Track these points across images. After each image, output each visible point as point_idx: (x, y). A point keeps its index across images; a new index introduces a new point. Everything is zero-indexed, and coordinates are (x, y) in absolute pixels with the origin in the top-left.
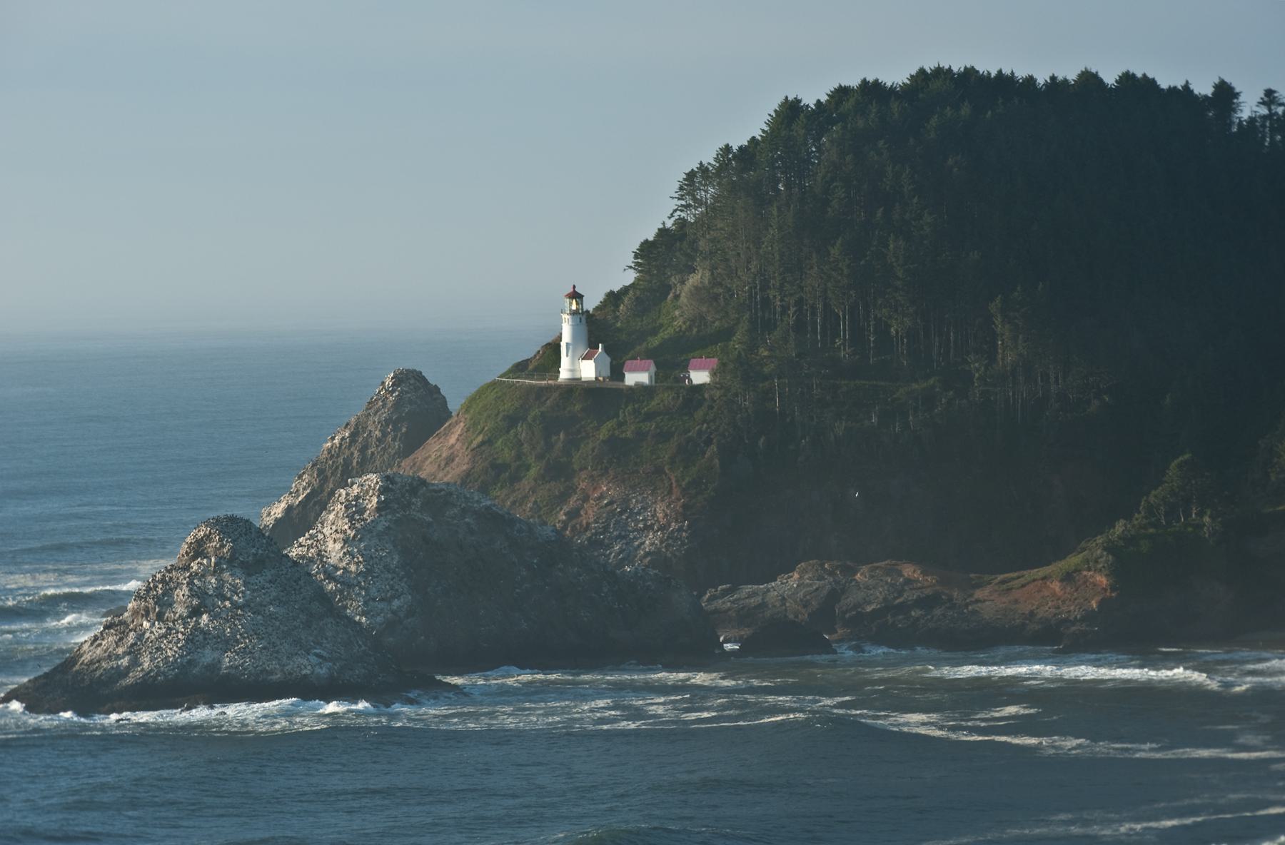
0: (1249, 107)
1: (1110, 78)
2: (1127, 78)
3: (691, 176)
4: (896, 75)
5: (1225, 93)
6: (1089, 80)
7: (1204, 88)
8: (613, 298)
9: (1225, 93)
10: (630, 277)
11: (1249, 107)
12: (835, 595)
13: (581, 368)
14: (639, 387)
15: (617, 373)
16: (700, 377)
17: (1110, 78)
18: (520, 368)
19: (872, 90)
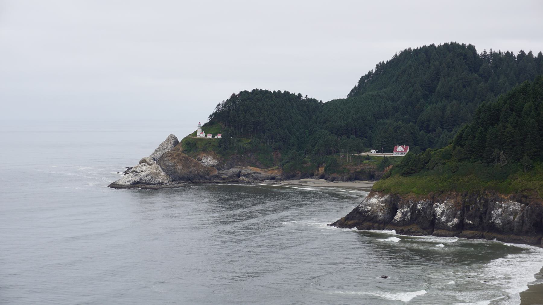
0: (303, 97)
1: (283, 92)
2: (285, 91)
3: (218, 105)
4: (250, 90)
5: (300, 95)
6: (279, 91)
7: (297, 94)
8: (205, 124)
9: (300, 95)
10: (208, 121)
11: (303, 97)
12: (240, 172)
13: (201, 135)
14: (209, 139)
15: (206, 136)
16: (219, 136)
17: (283, 92)
18: (190, 135)
19: (246, 92)
